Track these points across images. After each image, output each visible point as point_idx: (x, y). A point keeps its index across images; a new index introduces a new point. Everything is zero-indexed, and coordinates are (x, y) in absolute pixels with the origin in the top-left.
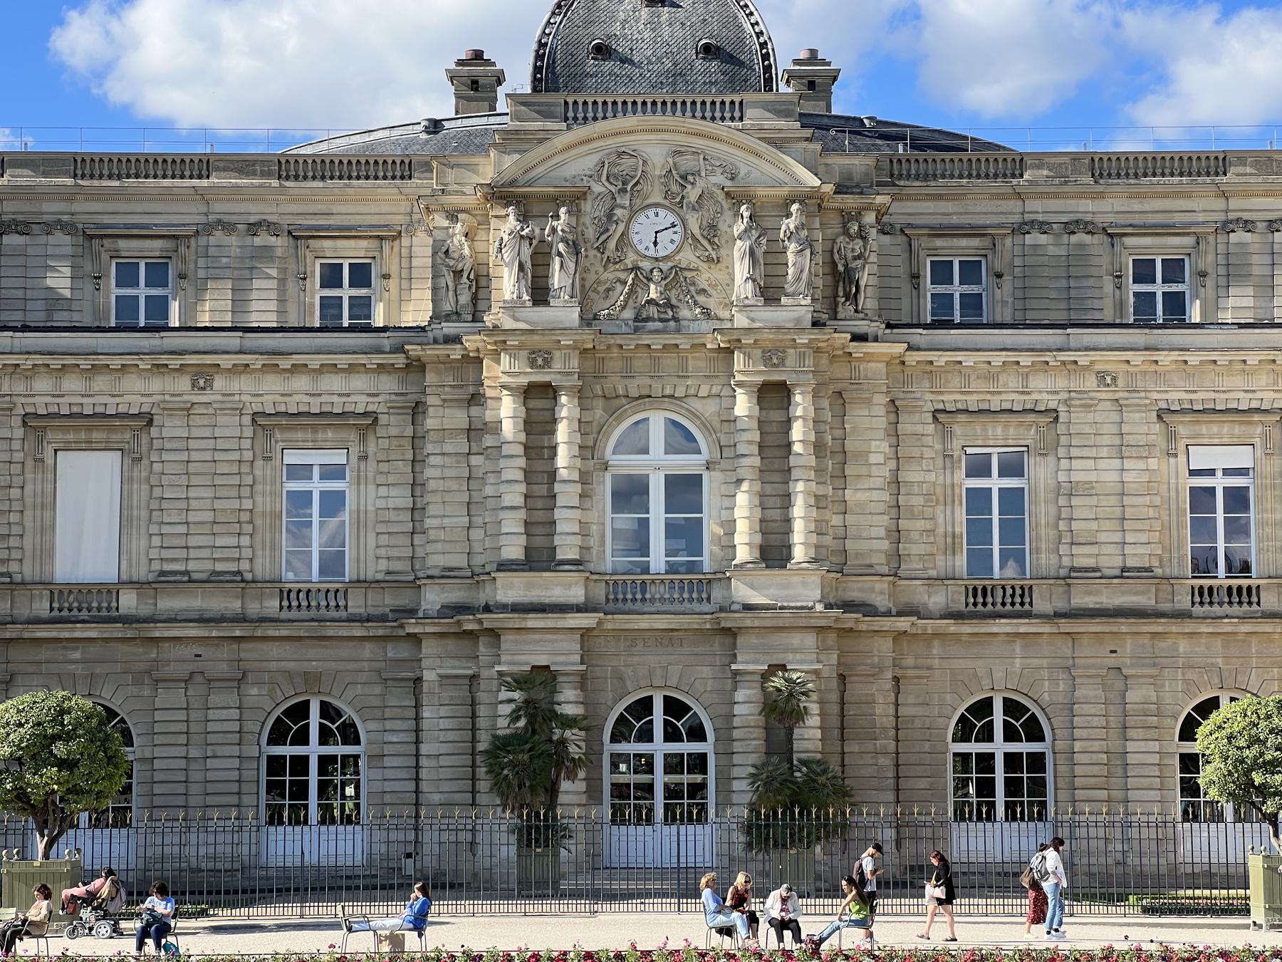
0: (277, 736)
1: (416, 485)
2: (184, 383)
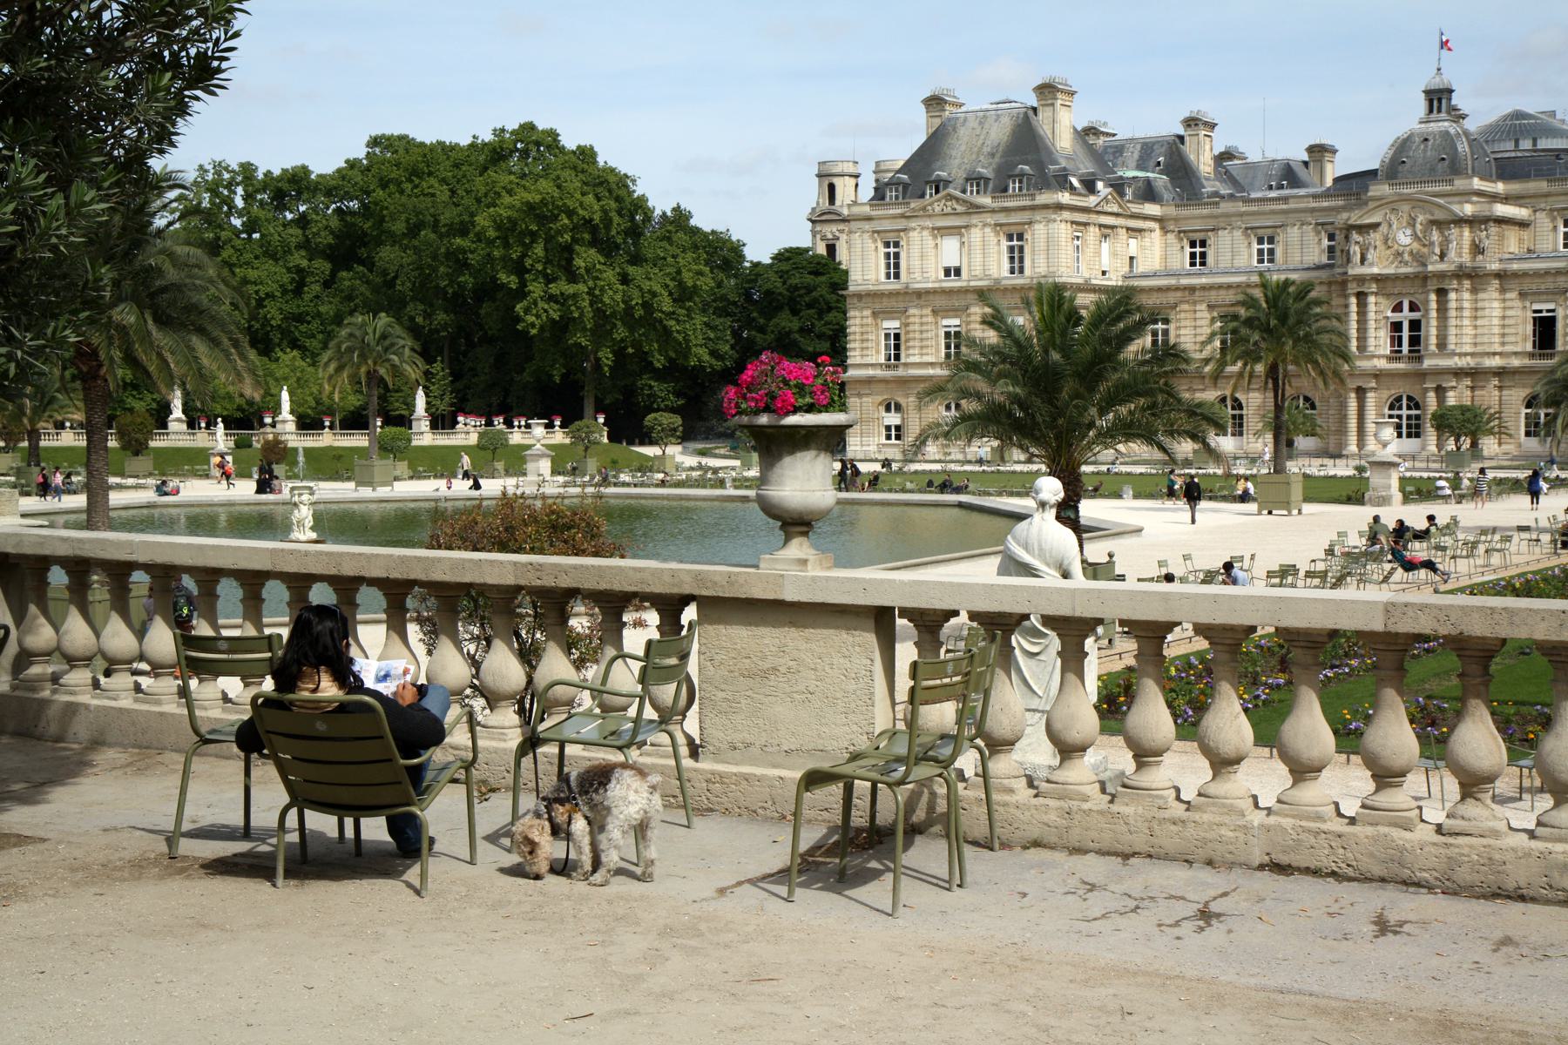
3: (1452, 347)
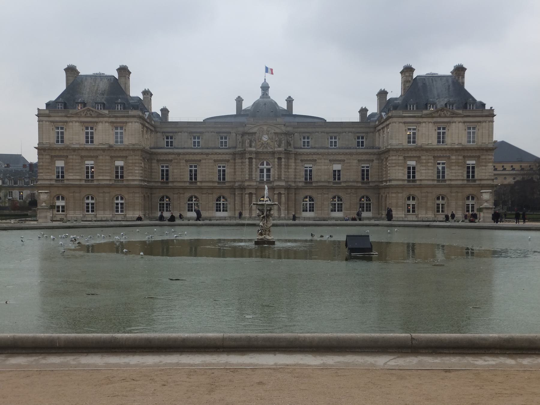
1: (235, 169)
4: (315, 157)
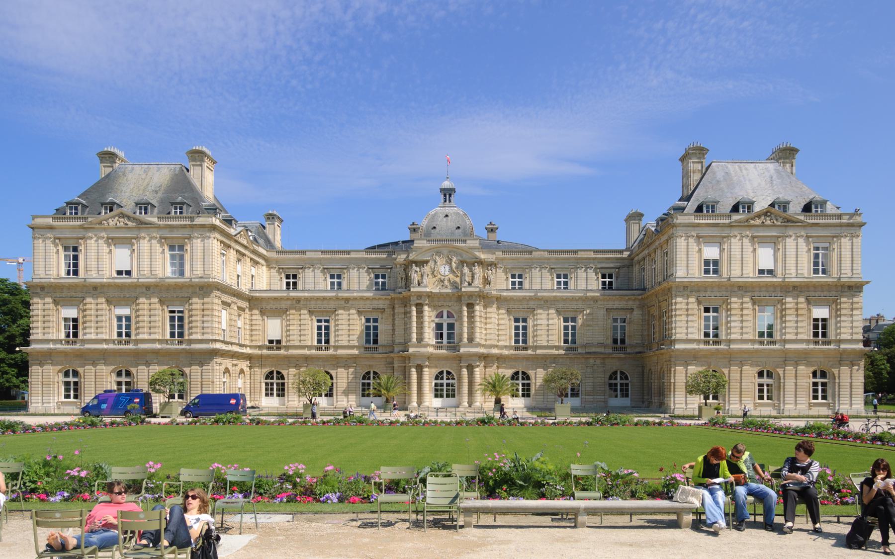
0: (364, 378)
1: (394, 325)
2: (343, 302)
3: (478, 340)
4: (532, 304)
